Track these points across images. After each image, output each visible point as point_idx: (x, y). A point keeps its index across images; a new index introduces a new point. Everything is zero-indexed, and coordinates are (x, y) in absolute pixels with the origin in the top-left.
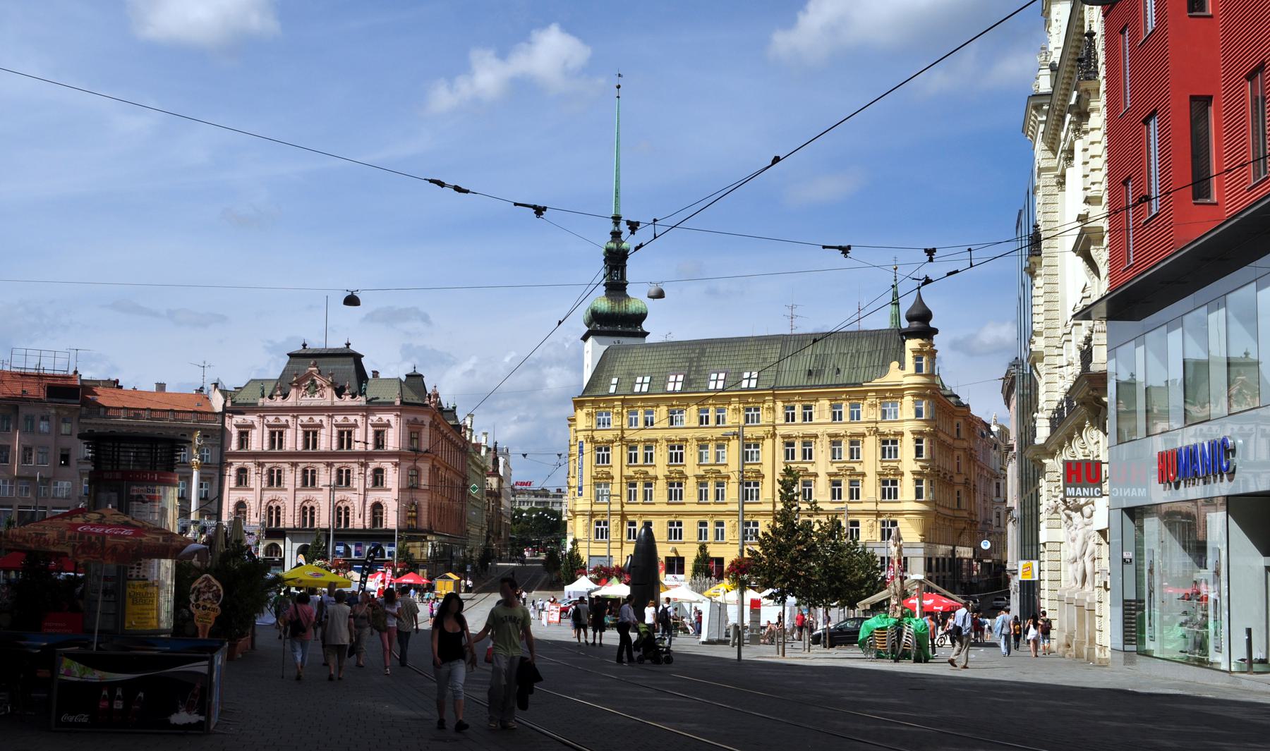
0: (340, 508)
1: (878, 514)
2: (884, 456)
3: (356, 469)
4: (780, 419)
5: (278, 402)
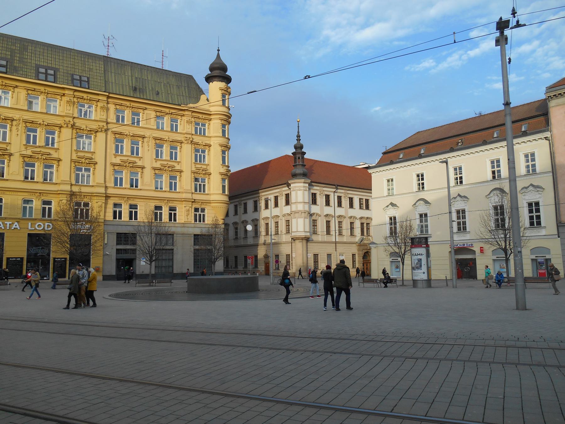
1: (194, 201)
2: (196, 160)
4: (112, 118)
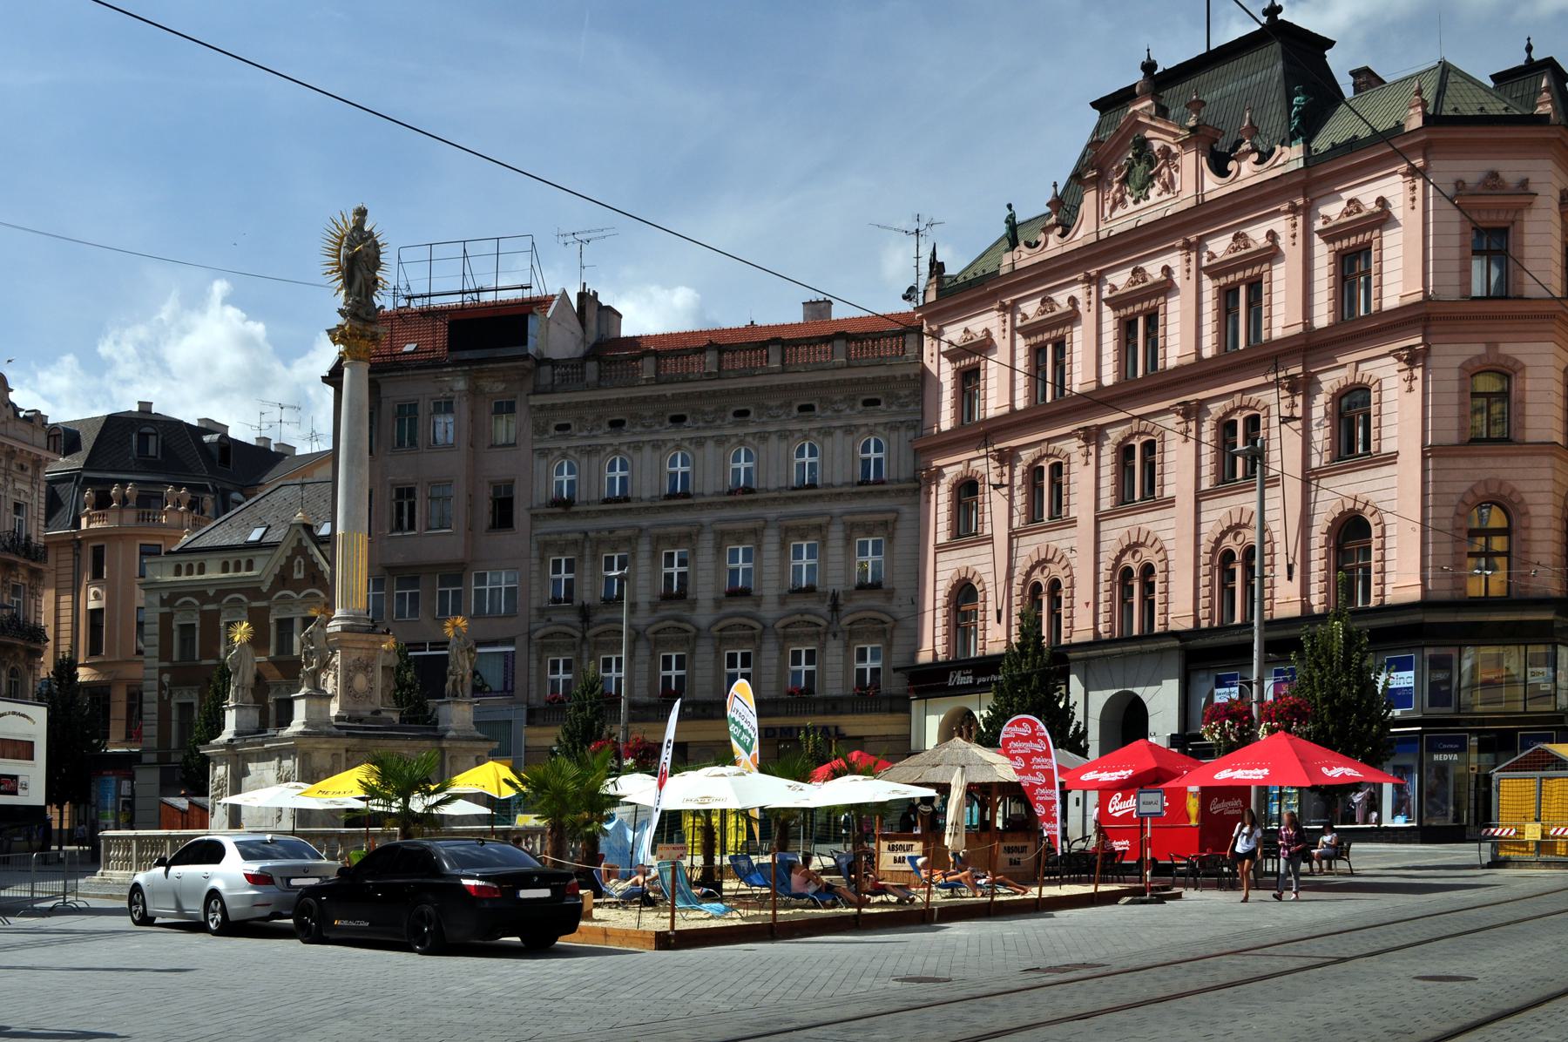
0: (1229, 556)
3: (1274, 402)
5: (1054, 246)
